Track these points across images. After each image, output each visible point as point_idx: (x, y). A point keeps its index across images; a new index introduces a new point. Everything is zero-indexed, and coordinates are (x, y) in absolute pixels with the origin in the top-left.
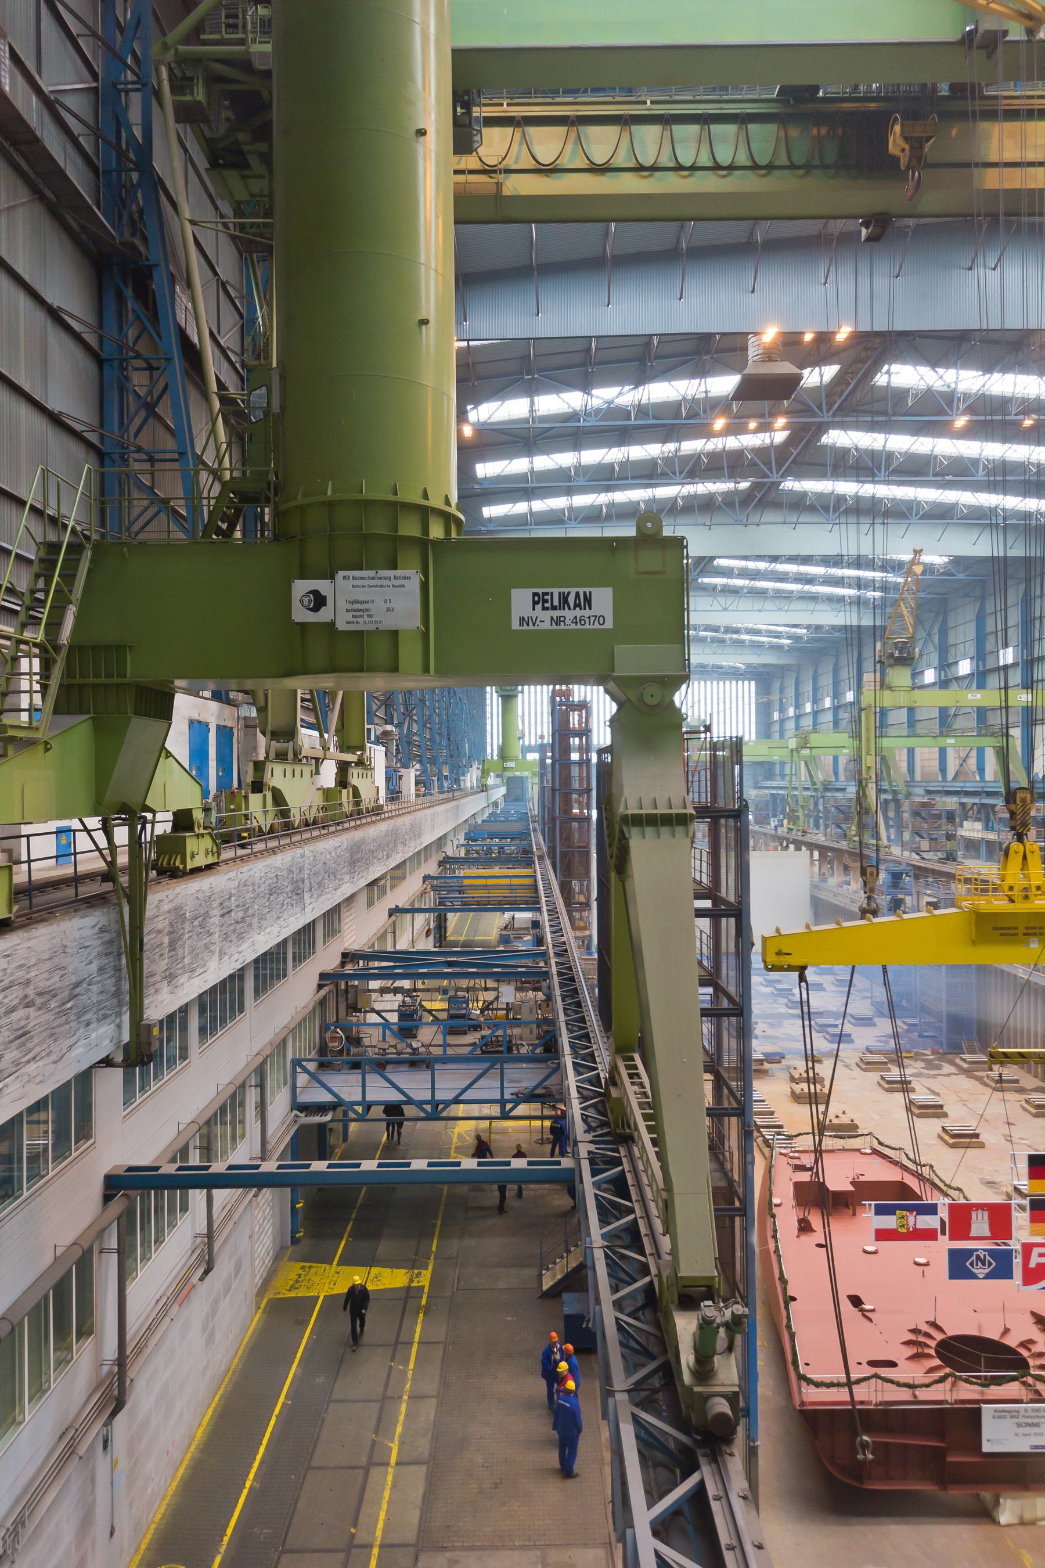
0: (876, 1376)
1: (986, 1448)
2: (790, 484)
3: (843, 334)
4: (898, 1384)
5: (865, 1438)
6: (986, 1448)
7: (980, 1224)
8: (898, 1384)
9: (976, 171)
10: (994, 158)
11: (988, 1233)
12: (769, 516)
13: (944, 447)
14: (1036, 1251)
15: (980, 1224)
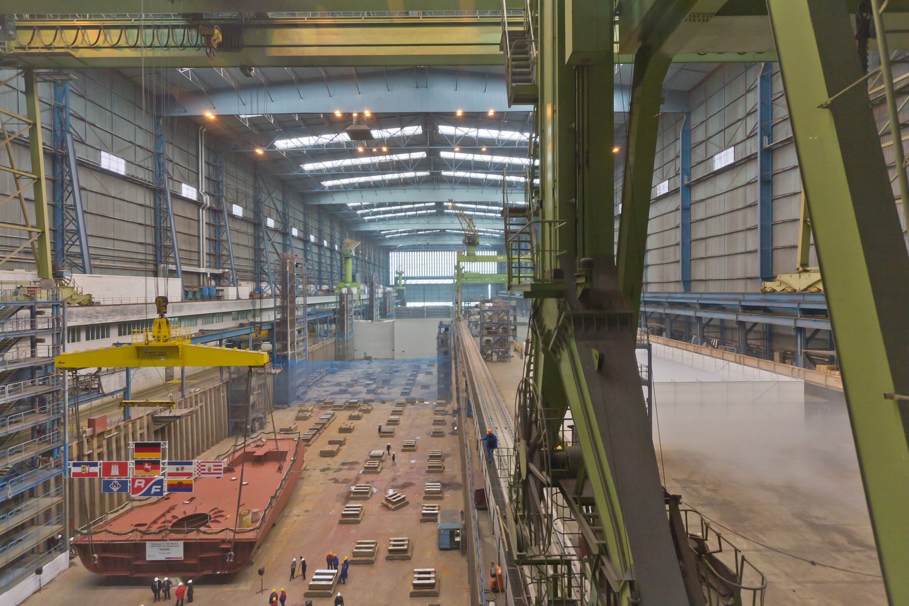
0: (137, 530)
1: (148, 559)
2: (444, 173)
3: (367, 114)
4: (114, 533)
5: (95, 555)
6: (148, 559)
7: (115, 471)
8: (114, 533)
9: (267, 49)
10: (273, 43)
11: (117, 473)
12: (442, 186)
13: (478, 157)
14: (137, 481)
15: (115, 471)
